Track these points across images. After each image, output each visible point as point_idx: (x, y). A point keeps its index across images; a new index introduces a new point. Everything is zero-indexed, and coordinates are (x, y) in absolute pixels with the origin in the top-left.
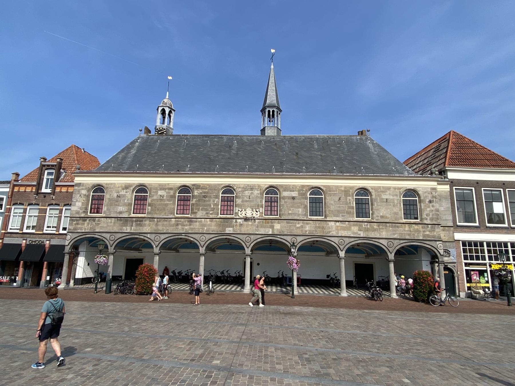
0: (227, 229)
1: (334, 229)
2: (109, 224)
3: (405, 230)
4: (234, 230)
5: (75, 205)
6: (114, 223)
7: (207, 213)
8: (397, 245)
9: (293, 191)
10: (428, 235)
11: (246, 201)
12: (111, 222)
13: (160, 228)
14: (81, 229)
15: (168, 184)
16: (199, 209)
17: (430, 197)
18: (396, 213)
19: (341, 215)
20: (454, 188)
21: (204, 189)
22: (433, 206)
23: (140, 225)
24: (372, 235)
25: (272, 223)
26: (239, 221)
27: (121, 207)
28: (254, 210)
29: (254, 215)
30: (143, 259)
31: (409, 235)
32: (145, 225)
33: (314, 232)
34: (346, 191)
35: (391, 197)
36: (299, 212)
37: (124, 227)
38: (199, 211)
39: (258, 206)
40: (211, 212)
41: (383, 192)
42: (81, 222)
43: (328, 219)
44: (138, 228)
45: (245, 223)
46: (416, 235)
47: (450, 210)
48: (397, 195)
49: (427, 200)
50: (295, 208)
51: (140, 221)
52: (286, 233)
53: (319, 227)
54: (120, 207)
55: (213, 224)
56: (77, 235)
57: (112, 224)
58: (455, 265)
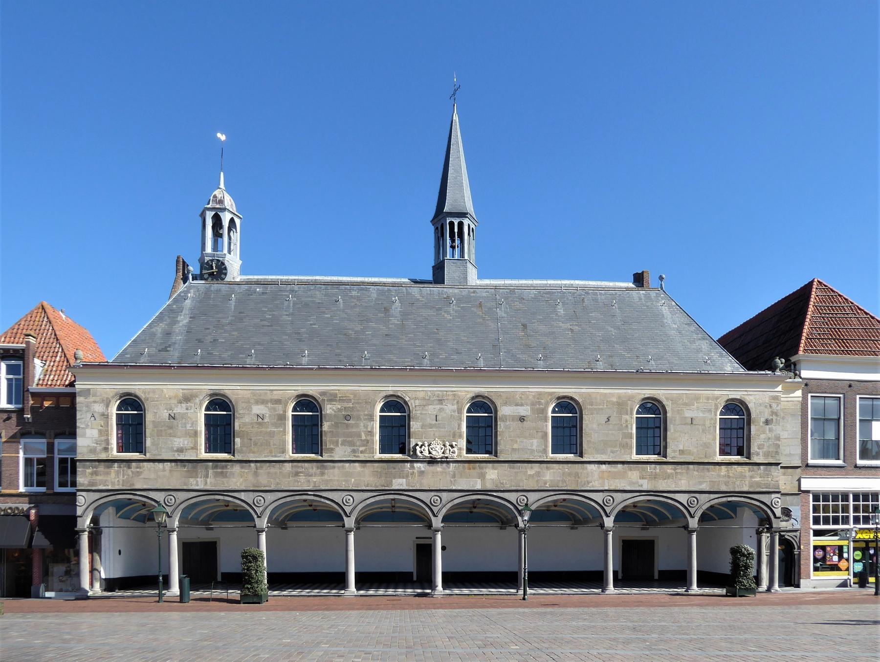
0: (394, 481)
1: (596, 477)
2: (161, 473)
3: (719, 476)
5: (84, 435)
6: (171, 471)
7: (354, 451)
8: (705, 502)
9: (522, 405)
10: (758, 484)
11: (431, 426)
12: (164, 470)
14: (105, 483)
16: (337, 442)
17: (767, 415)
18: (706, 445)
19: (609, 450)
20: (810, 395)
21: (343, 401)
23: (223, 475)
24: (662, 486)
27: (181, 440)
28: (447, 444)
31: (726, 484)
32: (233, 474)
33: (560, 485)
34: (621, 406)
35: (701, 415)
36: (532, 445)
37: (191, 480)
38: (337, 445)
39: (454, 436)
40: (361, 449)
41: (686, 404)
43: (584, 459)
44: (220, 480)
46: (738, 483)
48: (710, 411)
49: (763, 420)
50: (526, 438)
51: (223, 468)
52: (507, 487)
53: (570, 474)
56: (97, 495)
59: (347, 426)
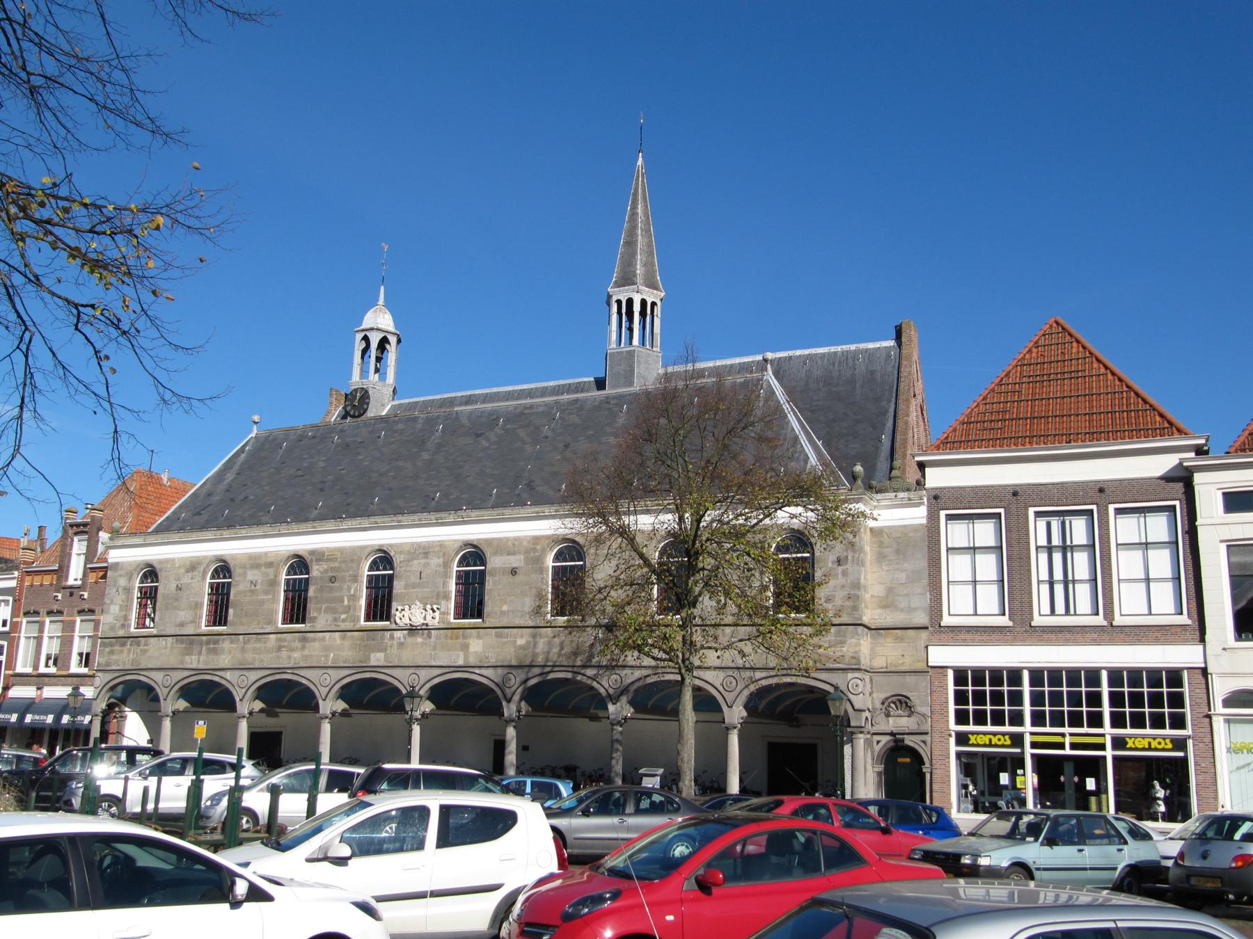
4: (386, 660)
5: (108, 612)
7: (335, 620)
9: (514, 554)
13: (249, 656)
14: (117, 662)
15: (266, 554)
22: (845, 573)
23: (214, 651)
25: (464, 637)
26: (398, 634)
28: (429, 607)
29: (429, 620)
30: (281, 733)
40: (343, 616)
42: (117, 648)
45: (410, 640)
47: (925, 581)
54: (181, 613)
55: (347, 643)
57: (168, 651)
58: (927, 738)
59: (331, 589)
